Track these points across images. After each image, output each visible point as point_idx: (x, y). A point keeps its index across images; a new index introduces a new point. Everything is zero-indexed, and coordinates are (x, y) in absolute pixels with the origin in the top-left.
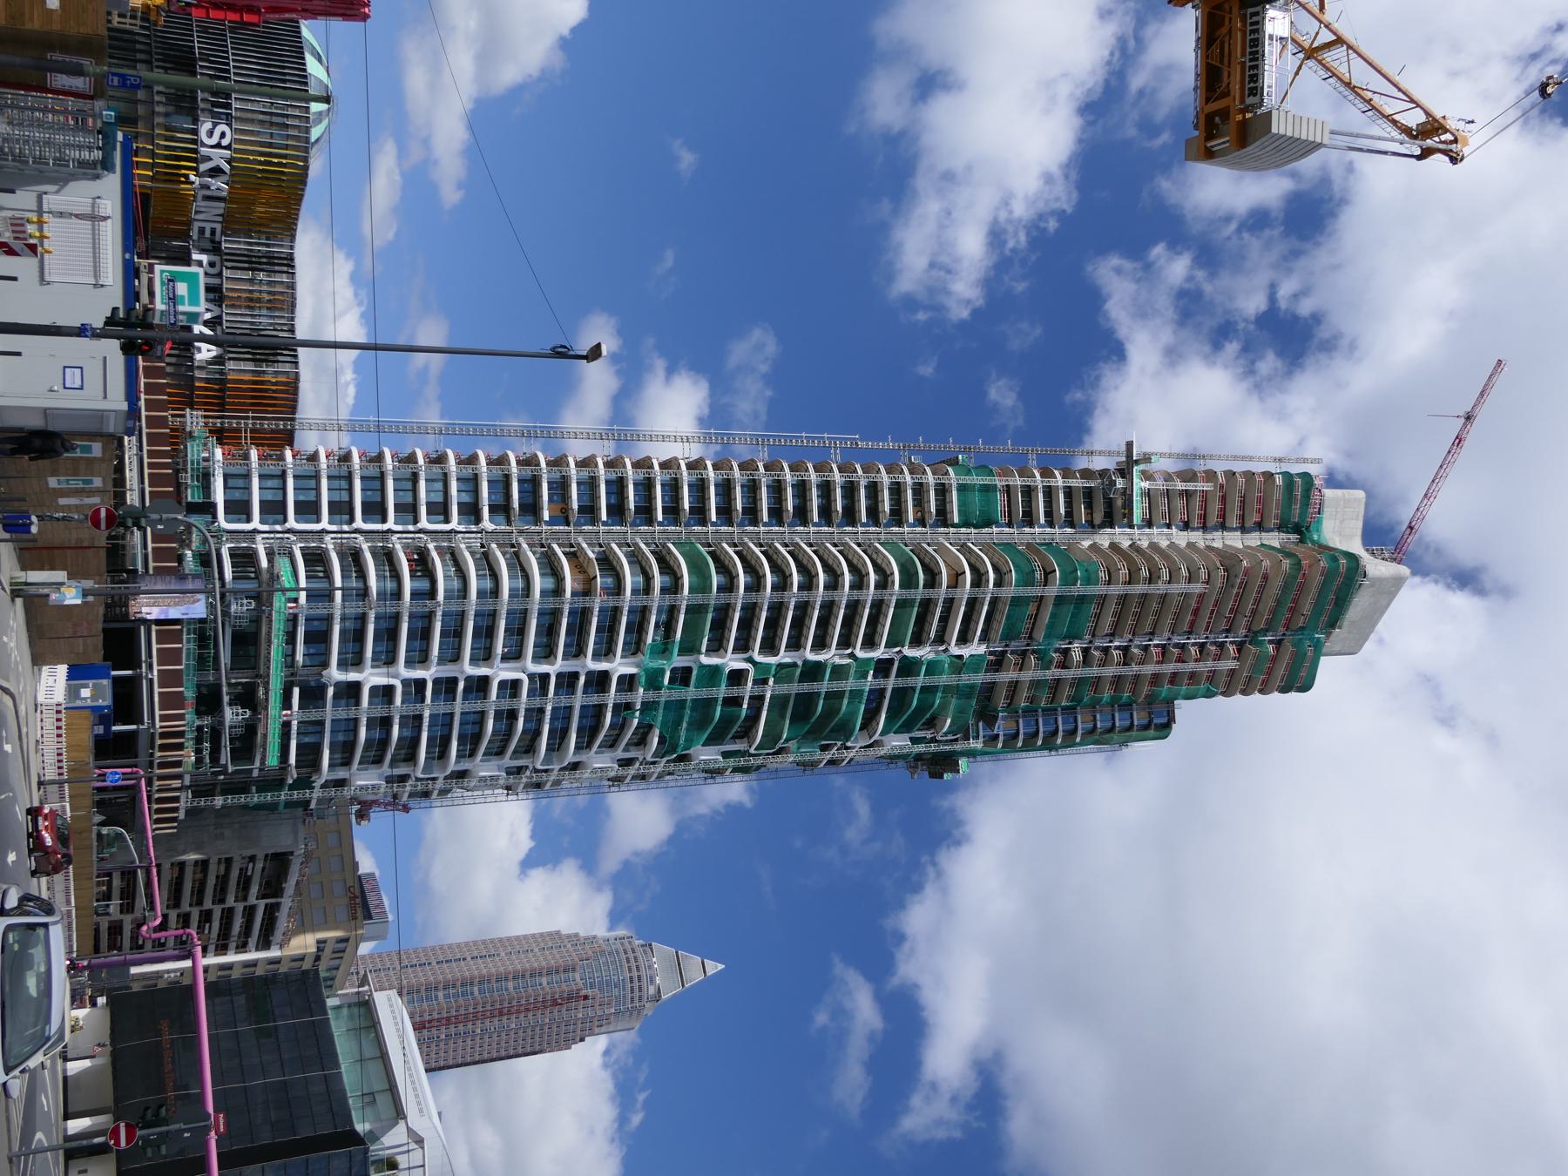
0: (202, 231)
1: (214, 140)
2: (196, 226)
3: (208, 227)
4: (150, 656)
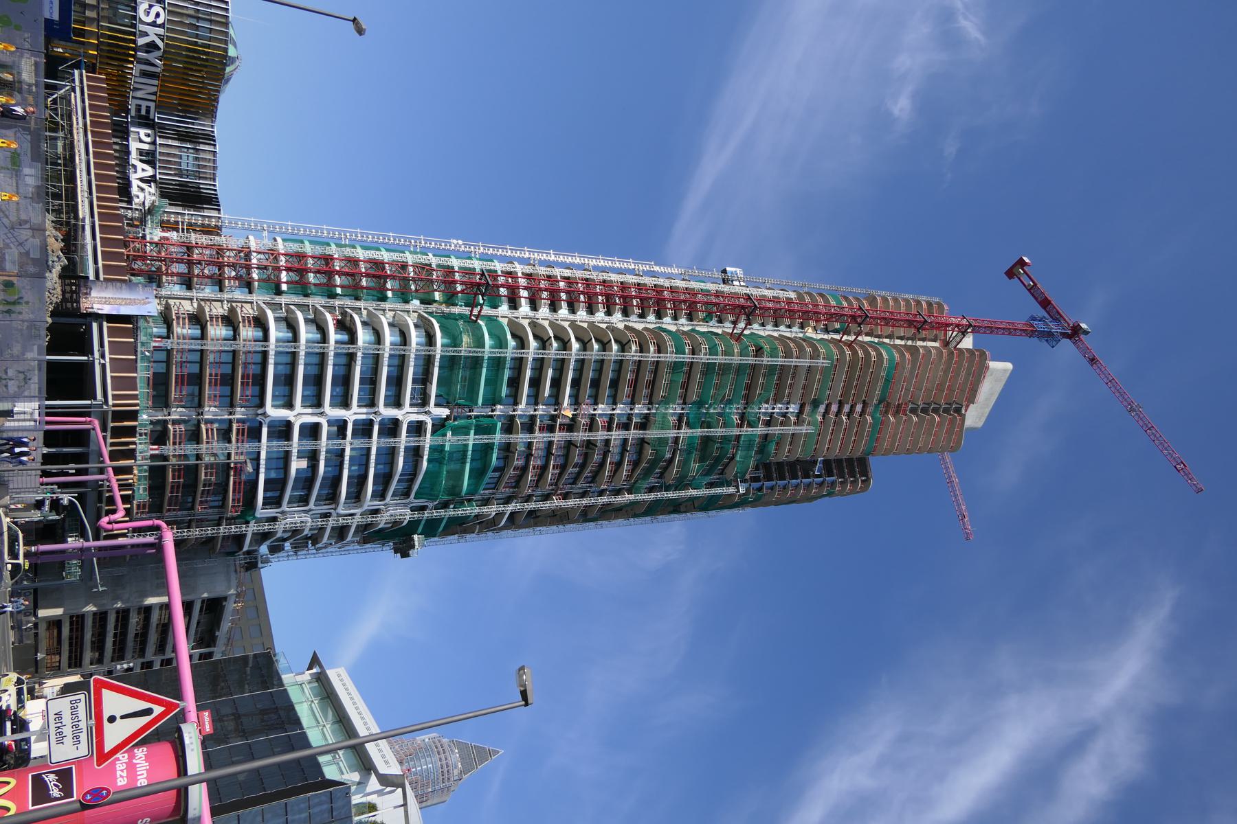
0: (139, 108)
1: (150, 19)
3: (144, 104)
4: (102, 345)
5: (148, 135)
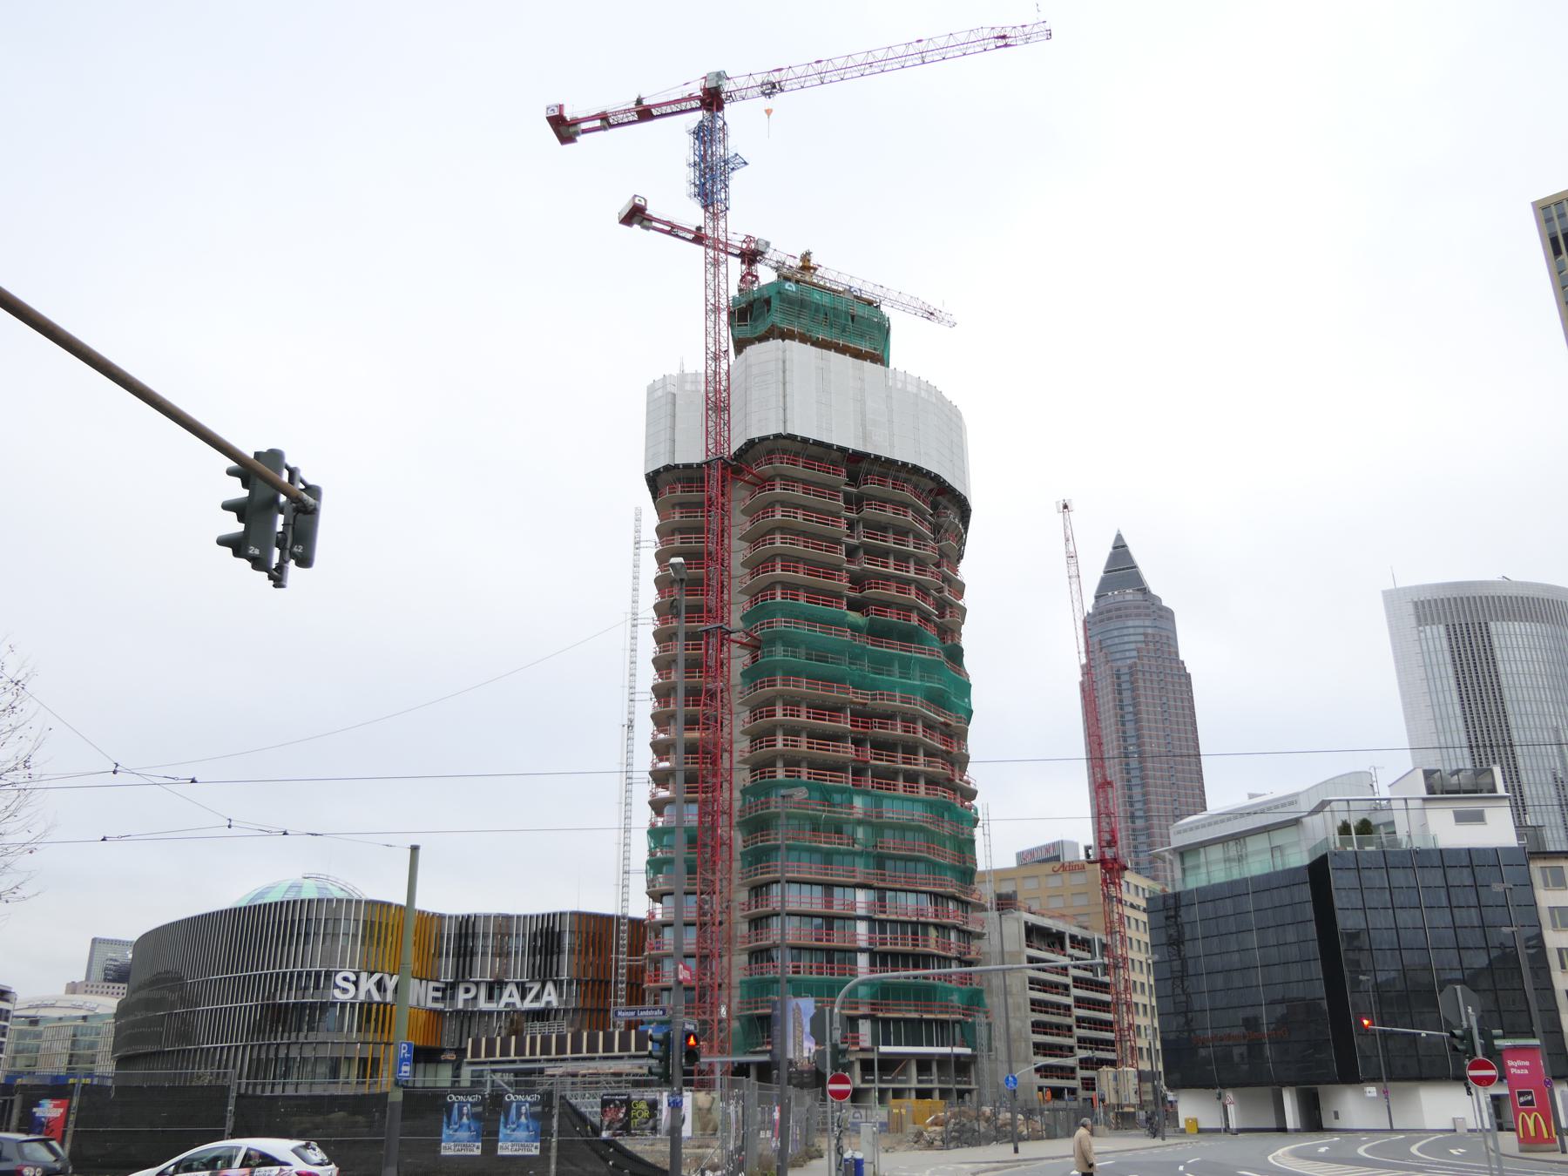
0: (435, 999)
1: (351, 987)
2: (430, 1005)
3: (432, 994)
5: (467, 991)
